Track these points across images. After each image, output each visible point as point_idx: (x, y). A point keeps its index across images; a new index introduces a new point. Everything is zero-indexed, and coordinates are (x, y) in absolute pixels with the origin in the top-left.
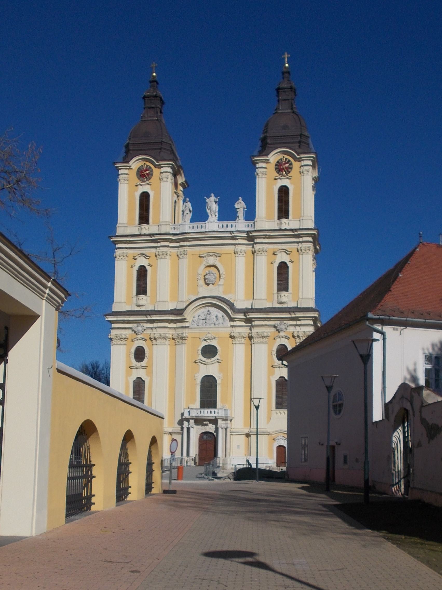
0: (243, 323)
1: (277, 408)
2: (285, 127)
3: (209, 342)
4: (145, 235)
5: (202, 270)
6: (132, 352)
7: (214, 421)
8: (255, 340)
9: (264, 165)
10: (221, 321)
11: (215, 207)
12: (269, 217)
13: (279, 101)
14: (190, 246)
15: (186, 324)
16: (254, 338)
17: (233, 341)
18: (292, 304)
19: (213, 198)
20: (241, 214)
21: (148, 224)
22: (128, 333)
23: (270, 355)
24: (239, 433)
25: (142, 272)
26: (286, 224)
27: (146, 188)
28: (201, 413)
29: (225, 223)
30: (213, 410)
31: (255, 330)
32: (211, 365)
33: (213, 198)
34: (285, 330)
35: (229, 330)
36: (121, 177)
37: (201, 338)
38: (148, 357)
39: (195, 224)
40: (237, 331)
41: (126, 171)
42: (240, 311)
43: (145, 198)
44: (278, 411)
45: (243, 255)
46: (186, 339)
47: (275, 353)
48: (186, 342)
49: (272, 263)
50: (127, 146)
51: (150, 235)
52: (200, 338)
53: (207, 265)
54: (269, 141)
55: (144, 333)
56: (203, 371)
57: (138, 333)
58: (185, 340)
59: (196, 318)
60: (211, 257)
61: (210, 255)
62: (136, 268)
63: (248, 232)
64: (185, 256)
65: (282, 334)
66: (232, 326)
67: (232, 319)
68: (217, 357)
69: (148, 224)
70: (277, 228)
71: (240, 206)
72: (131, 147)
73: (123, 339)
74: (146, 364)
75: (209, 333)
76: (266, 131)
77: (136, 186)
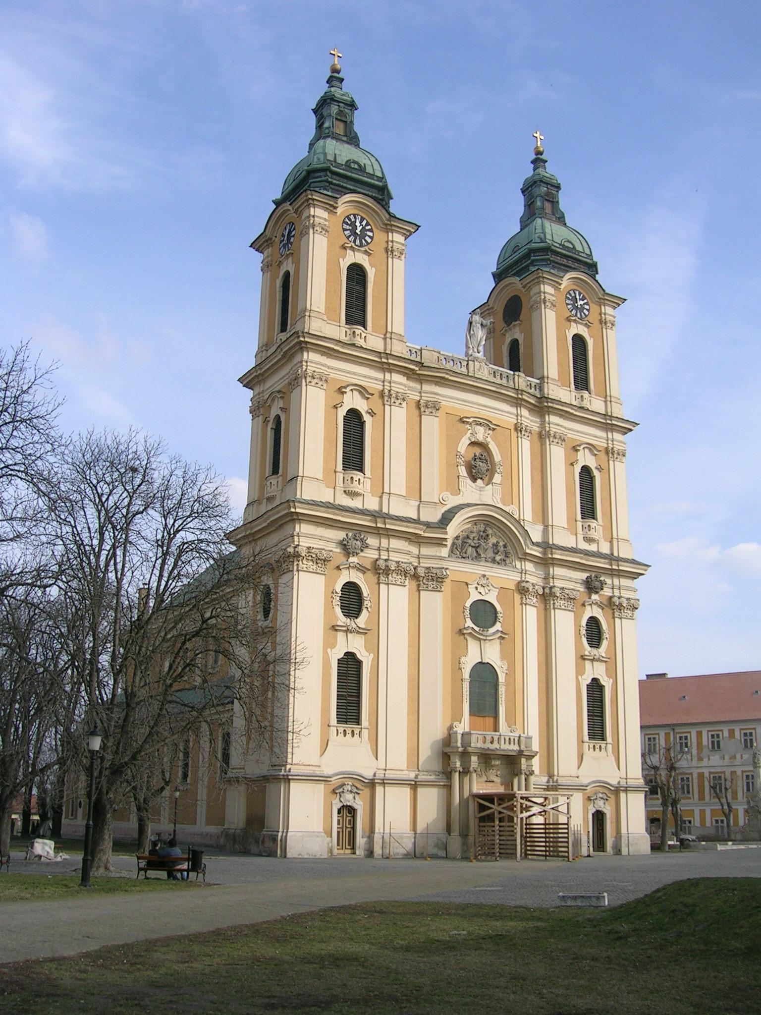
6: (336, 593)
17: (522, 598)
28: (492, 743)
43: (357, 274)
53: (473, 440)
60: (479, 427)
68: (498, 626)
73: (321, 560)
75: (484, 576)
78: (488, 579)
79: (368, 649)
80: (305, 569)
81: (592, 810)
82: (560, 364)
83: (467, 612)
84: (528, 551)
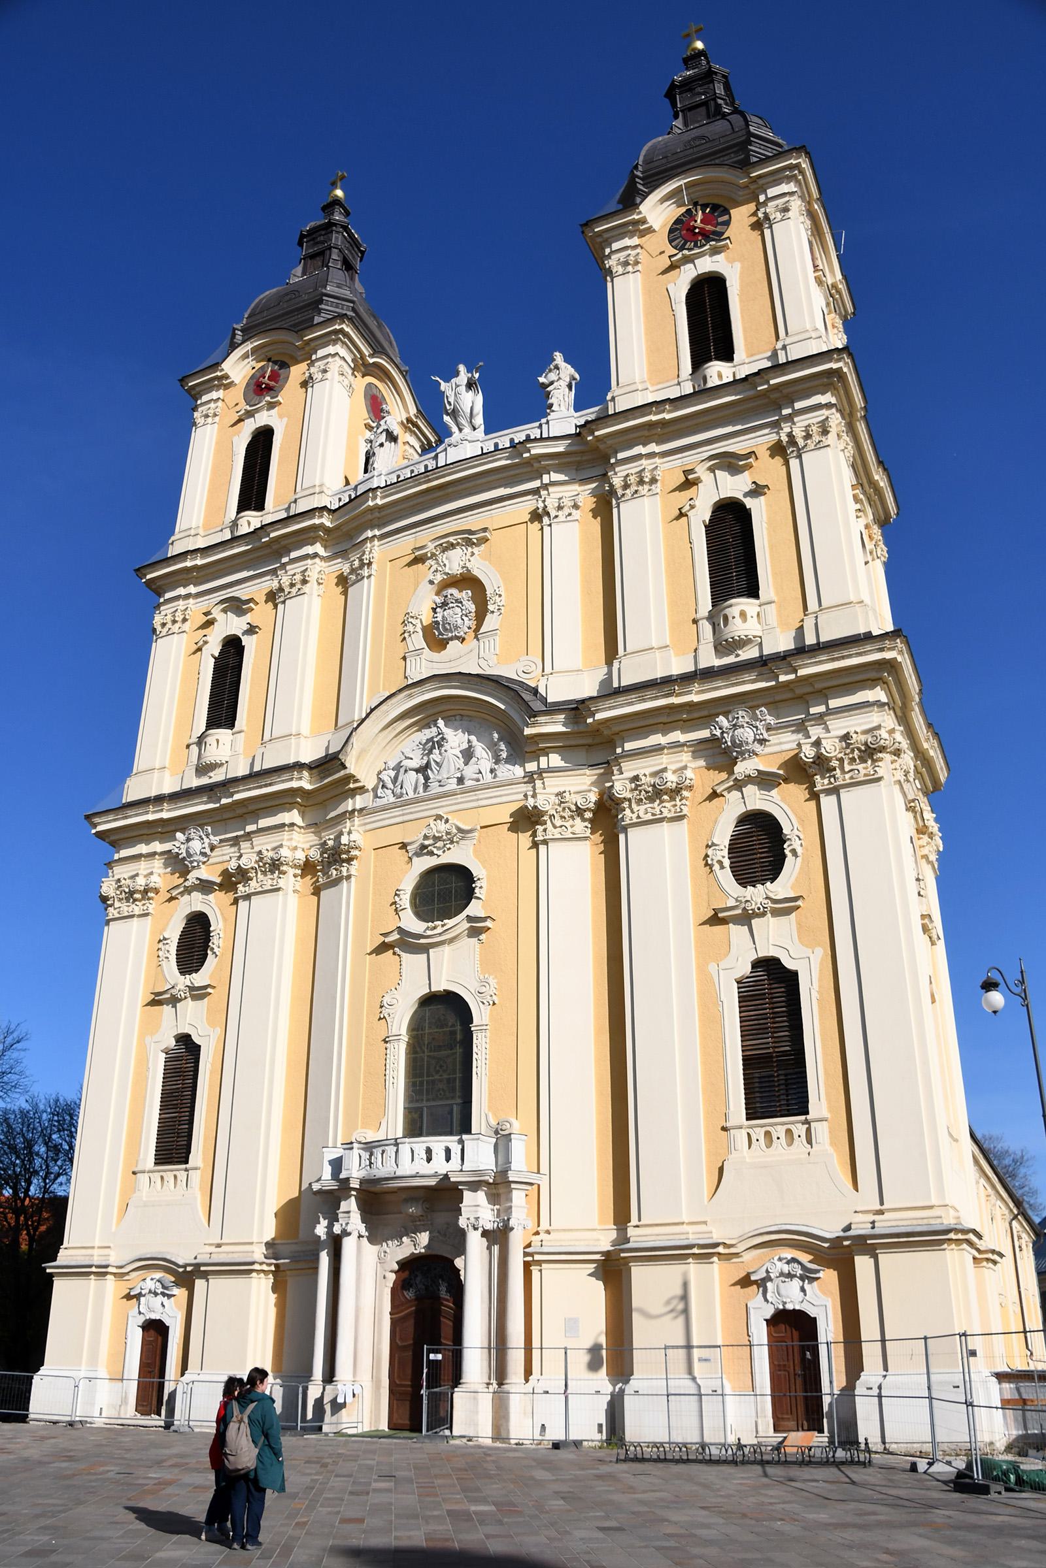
1: (753, 1113)
3: (439, 856)
5: (423, 605)
11: (472, 402)
15: (359, 801)
16: (626, 805)
22: (156, 874)
24: (570, 1258)
32: (446, 949)
33: (463, 376)
34: (757, 748)
37: (410, 844)
38: (216, 950)
44: (759, 1128)
45: (570, 514)
46: (355, 857)
47: (726, 852)
48: (355, 866)
49: (682, 515)
52: (404, 846)
53: (439, 578)
55: (211, 861)
57: (191, 862)
58: (349, 861)
60: (451, 553)
64: (365, 572)
74: (211, 977)
77: (240, 420)
78: (447, 821)
79: (212, 1023)
80: (118, 916)
81: (761, 1311)
82: (654, 349)
83: (405, 900)
84: (528, 731)
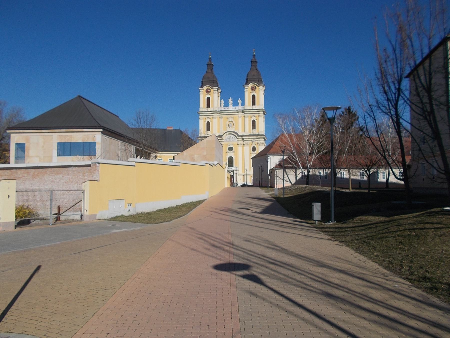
0: (241, 140)
2: (254, 75)
4: (209, 111)
5: (228, 123)
7: (233, 171)
8: (245, 145)
9: (247, 88)
10: (234, 139)
11: (231, 102)
12: (249, 105)
13: (252, 65)
14: (224, 115)
15: (223, 140)
18: (257, 134)
19: (231, 99)
20: (240, 104)
21: (210, 107)
23: (250, 150)
24: (241, 175)
25: (208, 123)
26: (254, 107)
27: (209, 96)
29: (235, 107)
30: (232, 168)
31: (245, 142)
33: (231, 99)
35: (237, 142)
36: (200, 92)
39: (225, 108)
40: (239, 143)
41: (202, 90)
42: (240, 136)
43: (208, 99)
50: (202, 82)
51: (210, 111)
54: (249, 80)
56: (229, 155)
59: (226, 138)
61: (230, 117)
62: (206, 122)
63: (242, 110)
65: (254, 143)
66: (238, 141)
67: (237, 139)
69: (210, 107)
70: (252, 109)
71: (240, 101)
72: (203, 82)
76: (247, 76)
